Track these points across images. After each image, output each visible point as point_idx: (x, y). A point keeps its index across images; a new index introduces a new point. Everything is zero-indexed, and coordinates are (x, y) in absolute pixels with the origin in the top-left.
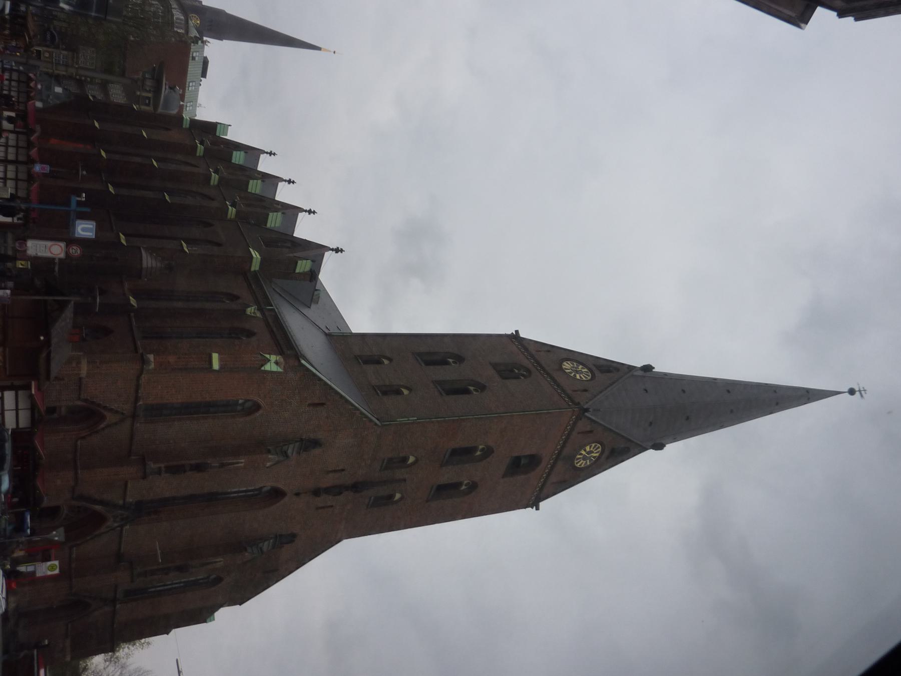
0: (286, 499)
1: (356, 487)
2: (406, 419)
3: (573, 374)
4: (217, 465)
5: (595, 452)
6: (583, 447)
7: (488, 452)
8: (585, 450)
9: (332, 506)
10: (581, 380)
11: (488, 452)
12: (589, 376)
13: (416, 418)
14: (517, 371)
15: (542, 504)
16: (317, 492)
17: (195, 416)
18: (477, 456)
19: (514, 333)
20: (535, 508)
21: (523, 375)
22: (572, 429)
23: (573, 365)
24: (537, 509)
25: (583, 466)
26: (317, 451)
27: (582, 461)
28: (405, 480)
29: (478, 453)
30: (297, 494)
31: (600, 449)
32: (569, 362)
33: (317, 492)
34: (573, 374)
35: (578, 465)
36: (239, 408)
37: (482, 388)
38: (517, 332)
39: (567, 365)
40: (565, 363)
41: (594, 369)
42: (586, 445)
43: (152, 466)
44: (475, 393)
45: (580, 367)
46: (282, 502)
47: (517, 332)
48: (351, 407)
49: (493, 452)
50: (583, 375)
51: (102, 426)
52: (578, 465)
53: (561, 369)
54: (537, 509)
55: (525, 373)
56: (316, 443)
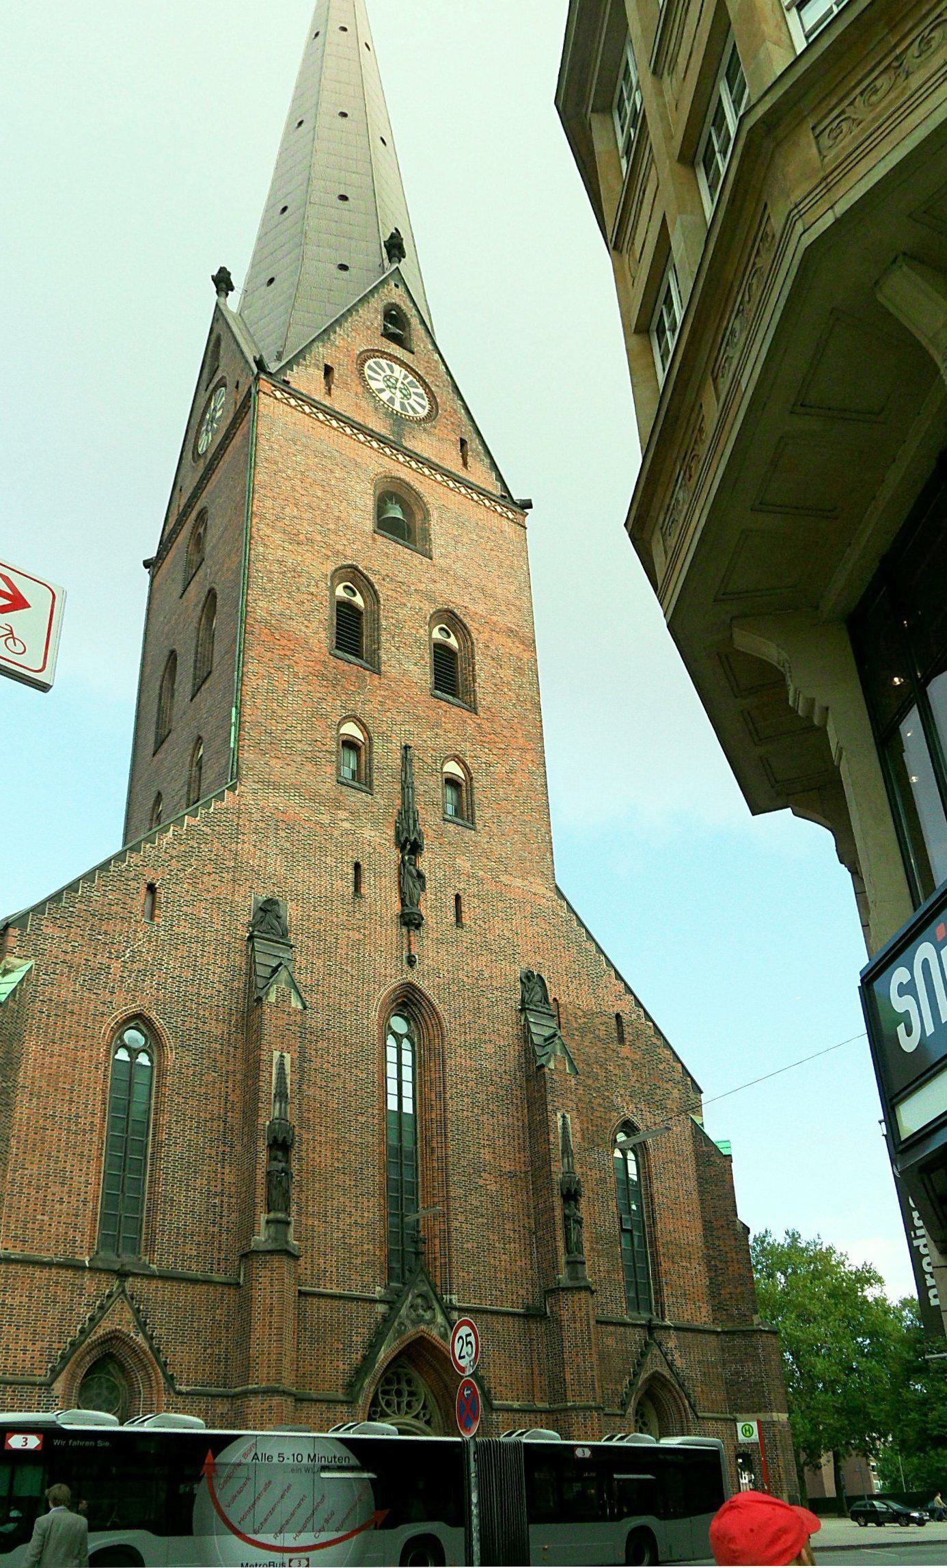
0: (423, 984)
1: (410, 846)
2: (233, 728)
4: (278, 1105)
5: (388, 372)
9: (458, 898)
13: (234, 709)
16: (410, 921)
17: (150, 1150)
25: (425, 403)
26: (291, 912)
27: (411, 401)
28: (407, 748)
30: (411, 962)
31: (383, 362)
33: (410, 921)
36: (143, 1059)
43: (261, 1237)
46: (428, 992)
48: (170, 834)
51: (140, 1339)
56: (268, 909)
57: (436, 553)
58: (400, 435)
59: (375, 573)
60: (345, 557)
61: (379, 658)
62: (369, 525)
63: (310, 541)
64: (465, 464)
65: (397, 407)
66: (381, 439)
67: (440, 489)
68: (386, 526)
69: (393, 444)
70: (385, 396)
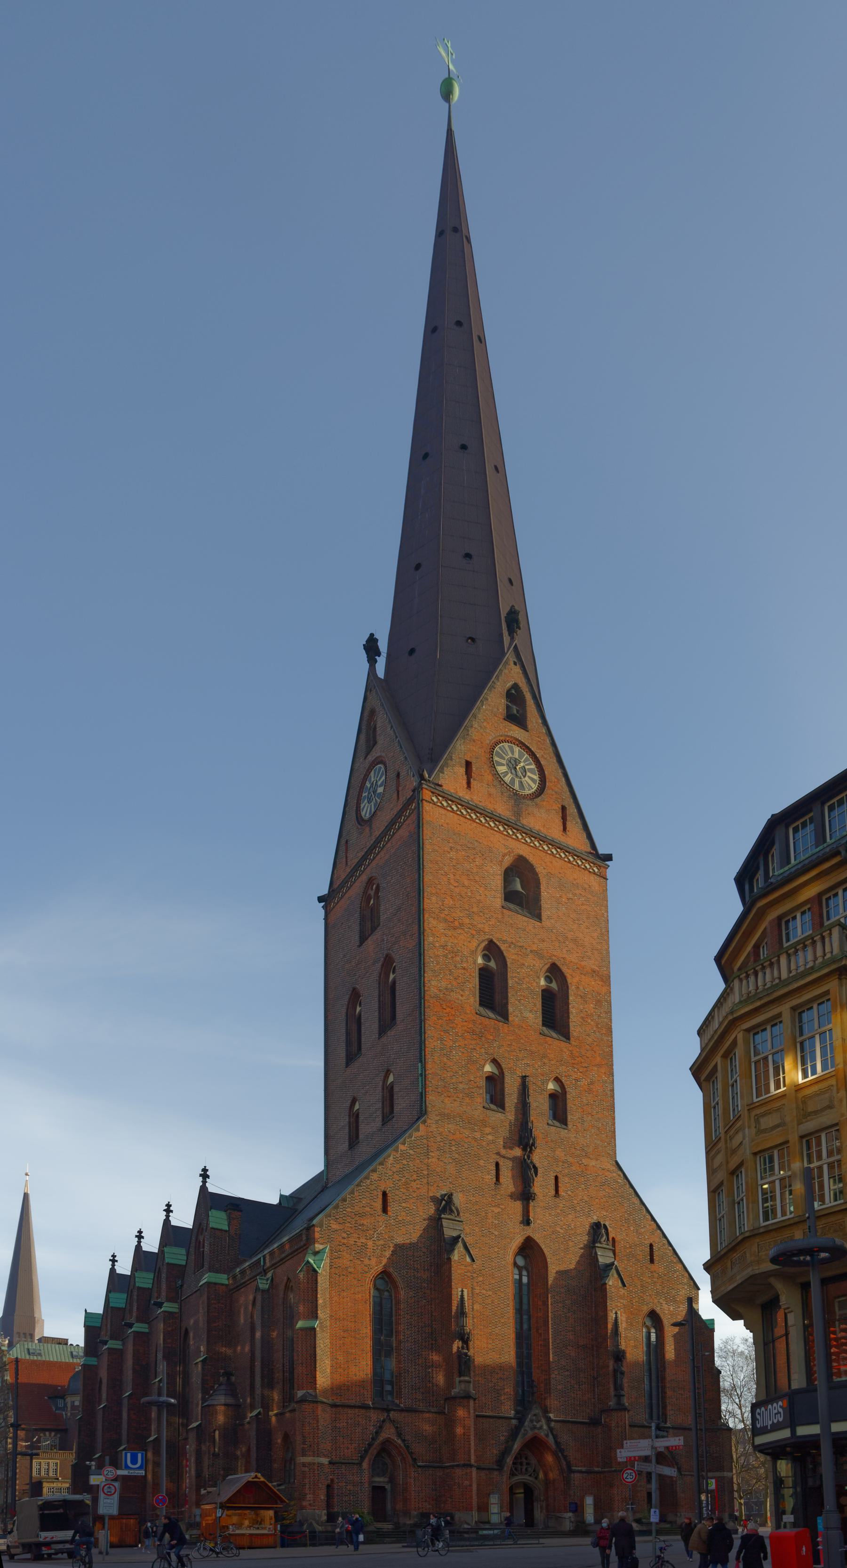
7: (492, 950)
8: (506, 774)
11: (492, 950)
14: (372, 902)
18: (497, 965)
19: (323, 904)
22: (459, 801)
25: (536, 777)
29: (492, 964)
37: (388, 963)
38: (320, 899)
39: (366, 810)
40: (363, 814)
47: (320, 899)
49: (491, 942)
52: (533, 785)
57: (544, 915)
58: (518, 814)
59: (504, 942)
60: (484, 932)
61: (507, 1011)
62: (498, 900)
63: (461, 924)
64: (565, 829)
65: (517, 786)
66: (506, 823)
67: (548, 858)
68: (510, 897)
69: (513, 825)
70: (508, 779)
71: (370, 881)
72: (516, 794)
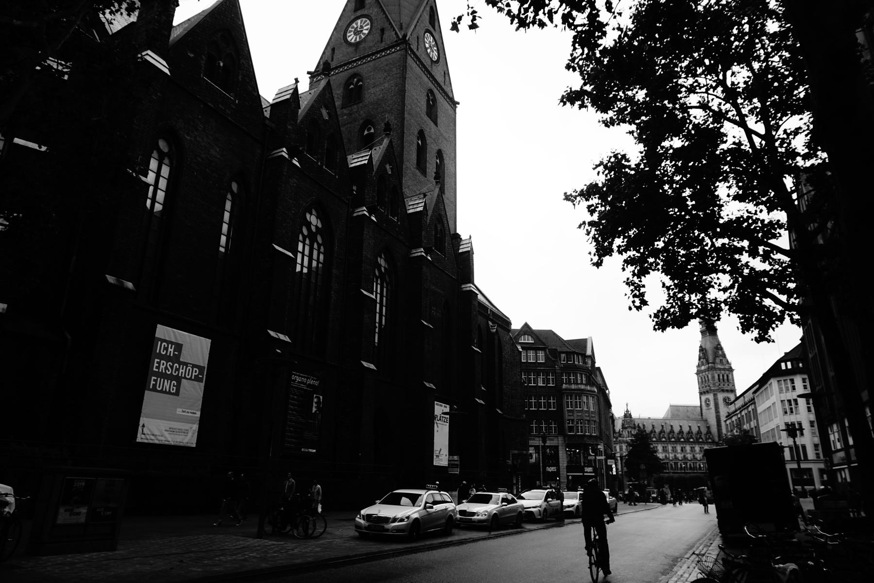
3: (362, 36)
6: (426, 49)
10: (371, 30)
12: (366, 21)
15: (456, 99)
19: (310, 75)
20: (457, 105)
21: (358, 81)
23: (352, 31)
24: (458, 103)
25: (437, 54)
31: (429, 35)
32: (348, 34)
34: (362, 36)
35: (436, 58)
38: (309, 73)
40: (349, 39)
41: (359, 13)
42: (425, 46)
44: (372, 131)
45: (435, 48)
47: (309, 73)
50: (364, 26)
53: (357, 45)
54: (458, 103)
55: (355, 80)
70: (429, 51)
71: (355, 75)
72: (431, 59)
